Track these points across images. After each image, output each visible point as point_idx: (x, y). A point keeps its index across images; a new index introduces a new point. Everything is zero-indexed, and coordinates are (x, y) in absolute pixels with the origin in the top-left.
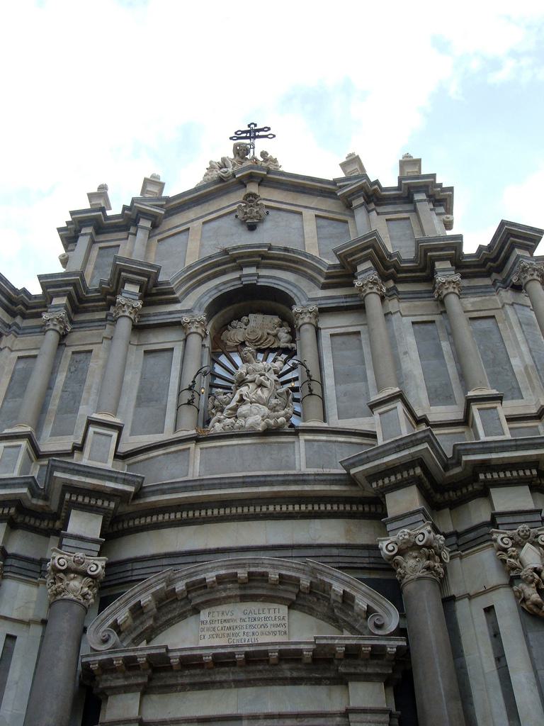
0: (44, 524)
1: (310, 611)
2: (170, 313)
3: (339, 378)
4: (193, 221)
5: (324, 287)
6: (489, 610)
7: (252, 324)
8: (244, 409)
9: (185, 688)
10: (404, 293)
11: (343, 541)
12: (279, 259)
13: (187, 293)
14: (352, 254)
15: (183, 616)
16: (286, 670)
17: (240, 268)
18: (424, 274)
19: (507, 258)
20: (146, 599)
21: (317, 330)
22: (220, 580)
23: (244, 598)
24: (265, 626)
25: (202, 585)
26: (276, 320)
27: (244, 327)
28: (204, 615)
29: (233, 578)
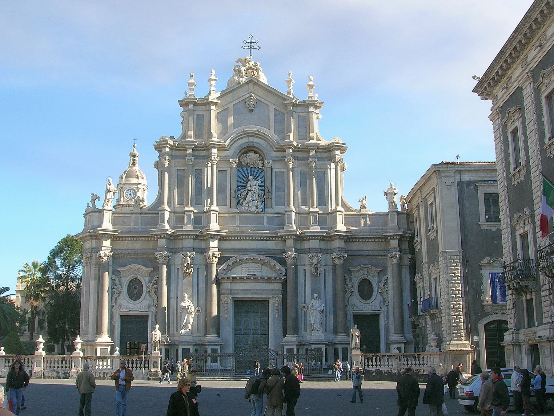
3: (277, 190)
4: (229, 103)
5: (275, 151)
7: (250, 157)
8: (250, 204)
10: (300, 157)
11: (274, 248)
12: (261, 135)
14: (286, 146)
16: (261, 281)
17: (248, 136)
18: (307, 150)
19: (333, 150)
20: (231, 264)
23: (251, 263)
24: (256, 270)
27: (248, 158)
29: (250, 259)
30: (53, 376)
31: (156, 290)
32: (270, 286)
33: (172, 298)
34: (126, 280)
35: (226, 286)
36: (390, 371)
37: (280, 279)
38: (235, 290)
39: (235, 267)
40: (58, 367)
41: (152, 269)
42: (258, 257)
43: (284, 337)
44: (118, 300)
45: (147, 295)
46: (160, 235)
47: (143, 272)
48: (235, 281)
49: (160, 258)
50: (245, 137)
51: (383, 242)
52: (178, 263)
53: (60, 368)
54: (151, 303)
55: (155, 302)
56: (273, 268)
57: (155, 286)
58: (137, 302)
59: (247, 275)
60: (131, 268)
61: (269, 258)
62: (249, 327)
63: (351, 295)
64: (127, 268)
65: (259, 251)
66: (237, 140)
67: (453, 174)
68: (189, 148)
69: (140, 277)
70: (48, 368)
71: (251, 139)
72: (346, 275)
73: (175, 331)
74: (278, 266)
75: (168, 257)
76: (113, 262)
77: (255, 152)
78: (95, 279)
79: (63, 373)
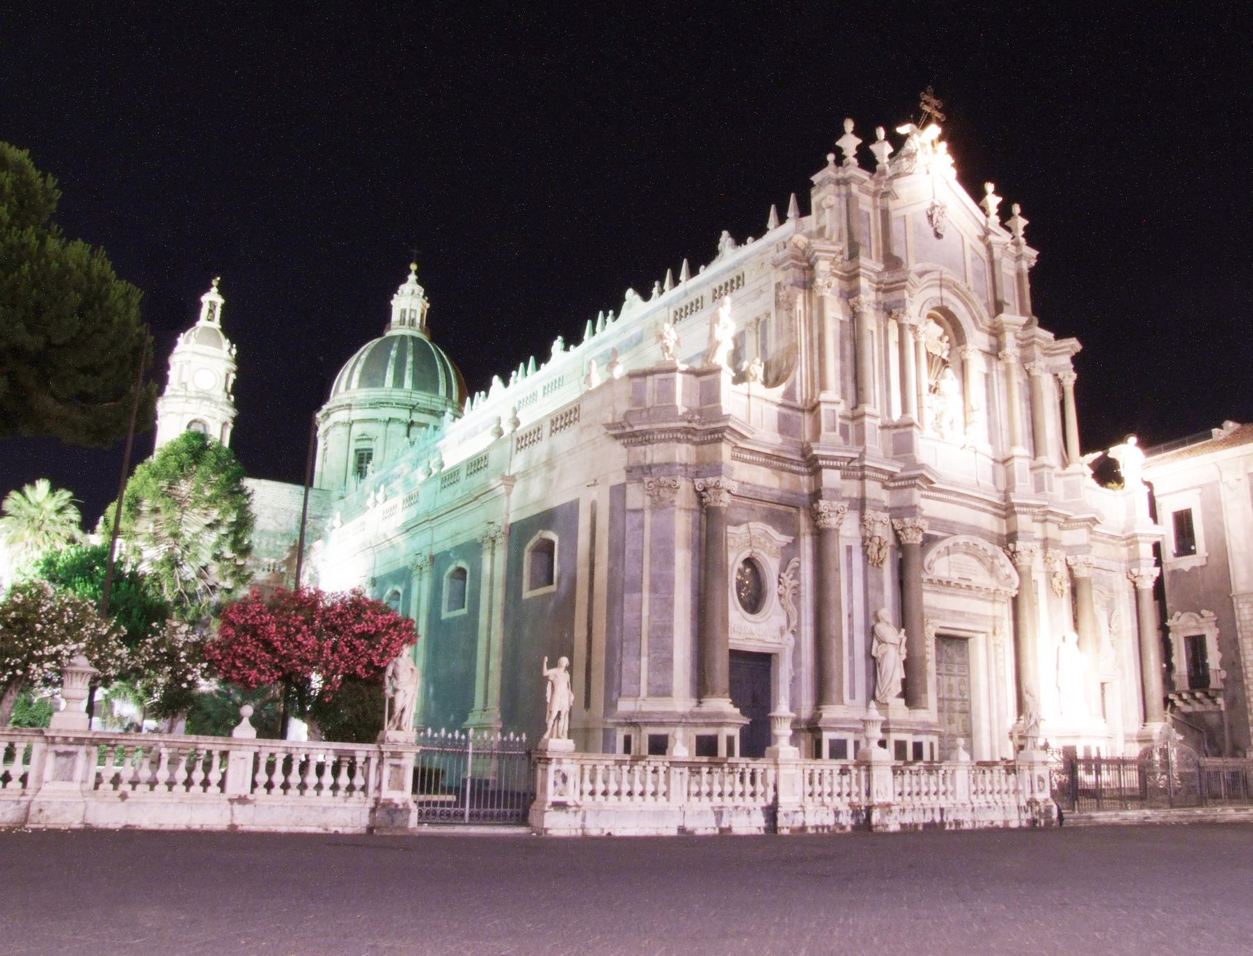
9: (947, 594)
23: (966, 553)
28: (951, 556)
30: (826, 823)
32: (985, 608)
35: (930, 599)
41: (790, 539)
49: (831, 514)
51: (1113, 544)
52: (848, 534)
54: (784, 623)
55: (794, 623)
56: (992, 571)
64: (743, 528)
65: (974, 530)
74: (1009, 568)
77: (938, 322)
79: (851, 812)
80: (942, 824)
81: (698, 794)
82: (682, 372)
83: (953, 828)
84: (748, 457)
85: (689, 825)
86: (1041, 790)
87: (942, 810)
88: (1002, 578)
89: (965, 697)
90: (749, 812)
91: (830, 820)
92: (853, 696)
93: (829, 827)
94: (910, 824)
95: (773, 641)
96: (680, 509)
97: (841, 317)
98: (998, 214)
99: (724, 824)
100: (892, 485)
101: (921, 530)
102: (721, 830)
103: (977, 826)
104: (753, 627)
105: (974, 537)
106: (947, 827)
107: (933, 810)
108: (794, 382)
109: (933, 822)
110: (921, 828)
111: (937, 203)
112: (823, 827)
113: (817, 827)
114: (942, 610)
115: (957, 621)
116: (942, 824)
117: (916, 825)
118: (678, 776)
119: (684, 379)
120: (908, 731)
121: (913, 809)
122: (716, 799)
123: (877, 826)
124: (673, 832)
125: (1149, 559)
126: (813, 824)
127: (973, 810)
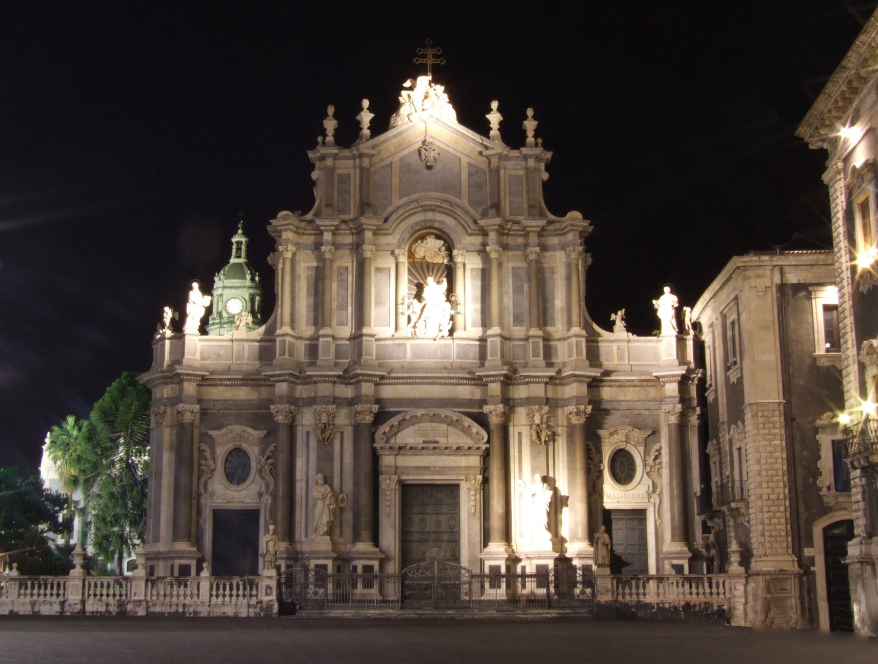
0: (346, 381)
1: (456, 427)
2: (387, 245)
5: (470, 235)
6: (520, 433)
7: (429, 245)
9: (410, 455)
12: (447, 209)
13: (395, 229)
15: (408, 426)
17: (425, 211)
21: (464, 265)
22: (422, 415)
23: (431, 421)
25: (416, 416)
26: (442, 242)
28: (416, 427)
30: (100, 610)
31: (272, 467)
32: (463, 461)
33: (299, 481)
34: (221, 451)
35: (387, 460)
36: (661, 605)
37: (478, 448)
38: (404, 467)
39: (403, 429)
40: (108, 595)
41: (265, 432)
42: (443, 412)
43: (485, 545)
44: (210, 485)
45: (257, 475)
46: (279, 375)
47: (251, 438)
48: (402, 452)
50: (420, 212)
51: (652, 386)
52: (308, 423)
53: (111, 598)
54: (263, 489)
55: (272, 487)
56: (466, 431)
57: (270, 461)
58: (240, 487)
59: (424, 442)
60: (231, 431)
61: (461, 415)
62: (427, 530)
63: (598, 476)
64: (224, 430)
66: (407, 217)
67: (768, 273)
68: (326, 231)
69: (245, 446)
70: (92, 597)
71: (430, 215)
72: (589, 443)
73: (303, 536)
74: (476, 428)
75: (292, 413)
76: (201, 421)
77: (438, 237)
78: (171, 448)
80: (184, 612)
81: (25, 595)
82: (169, 339)
83: (192, 615)
84: (228, 382)
85: (16, 609)
86: (267, 594)
87: (184, 605)
88: (474, 435)
89: (455, 530)
90: (51, 604)
91: (103, 609)
92: (306, 536)
93: (101, 612)
94: (159, 613)
95: (251, 501)
96: (167, 426)
97: (315, 264)
98: (499, 130)
99: (36, 609)
100: (352, 381)
101: (371, 412)
102: (34, 612)
103: (211, 615)
104: (235, 494)
105: (433, 409)
106: (188, 615)
107: (177, 605)
108: (275, 320)
109: (177, 612)
110: (166, 615)
111: (429, 140)
112: (97, 612)
113: (93, 612)
114: (408, 467)
115: (422, 474)
116: (184, 612)
117: (163, 613)
118: (13, 585)
119: (171, 343)
120: (326, 558)
121: (162, 604)
122: (35, 597)
123: (130, 612)
124: (7, 613)
125: (675, 397)
126: (91, 610)
127: (209, 605)
